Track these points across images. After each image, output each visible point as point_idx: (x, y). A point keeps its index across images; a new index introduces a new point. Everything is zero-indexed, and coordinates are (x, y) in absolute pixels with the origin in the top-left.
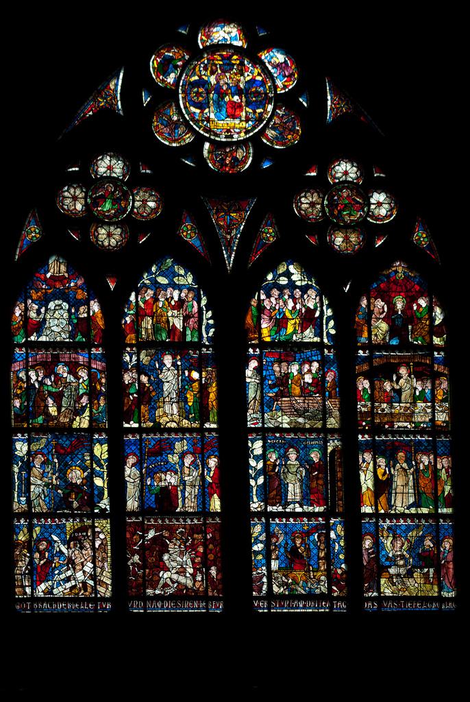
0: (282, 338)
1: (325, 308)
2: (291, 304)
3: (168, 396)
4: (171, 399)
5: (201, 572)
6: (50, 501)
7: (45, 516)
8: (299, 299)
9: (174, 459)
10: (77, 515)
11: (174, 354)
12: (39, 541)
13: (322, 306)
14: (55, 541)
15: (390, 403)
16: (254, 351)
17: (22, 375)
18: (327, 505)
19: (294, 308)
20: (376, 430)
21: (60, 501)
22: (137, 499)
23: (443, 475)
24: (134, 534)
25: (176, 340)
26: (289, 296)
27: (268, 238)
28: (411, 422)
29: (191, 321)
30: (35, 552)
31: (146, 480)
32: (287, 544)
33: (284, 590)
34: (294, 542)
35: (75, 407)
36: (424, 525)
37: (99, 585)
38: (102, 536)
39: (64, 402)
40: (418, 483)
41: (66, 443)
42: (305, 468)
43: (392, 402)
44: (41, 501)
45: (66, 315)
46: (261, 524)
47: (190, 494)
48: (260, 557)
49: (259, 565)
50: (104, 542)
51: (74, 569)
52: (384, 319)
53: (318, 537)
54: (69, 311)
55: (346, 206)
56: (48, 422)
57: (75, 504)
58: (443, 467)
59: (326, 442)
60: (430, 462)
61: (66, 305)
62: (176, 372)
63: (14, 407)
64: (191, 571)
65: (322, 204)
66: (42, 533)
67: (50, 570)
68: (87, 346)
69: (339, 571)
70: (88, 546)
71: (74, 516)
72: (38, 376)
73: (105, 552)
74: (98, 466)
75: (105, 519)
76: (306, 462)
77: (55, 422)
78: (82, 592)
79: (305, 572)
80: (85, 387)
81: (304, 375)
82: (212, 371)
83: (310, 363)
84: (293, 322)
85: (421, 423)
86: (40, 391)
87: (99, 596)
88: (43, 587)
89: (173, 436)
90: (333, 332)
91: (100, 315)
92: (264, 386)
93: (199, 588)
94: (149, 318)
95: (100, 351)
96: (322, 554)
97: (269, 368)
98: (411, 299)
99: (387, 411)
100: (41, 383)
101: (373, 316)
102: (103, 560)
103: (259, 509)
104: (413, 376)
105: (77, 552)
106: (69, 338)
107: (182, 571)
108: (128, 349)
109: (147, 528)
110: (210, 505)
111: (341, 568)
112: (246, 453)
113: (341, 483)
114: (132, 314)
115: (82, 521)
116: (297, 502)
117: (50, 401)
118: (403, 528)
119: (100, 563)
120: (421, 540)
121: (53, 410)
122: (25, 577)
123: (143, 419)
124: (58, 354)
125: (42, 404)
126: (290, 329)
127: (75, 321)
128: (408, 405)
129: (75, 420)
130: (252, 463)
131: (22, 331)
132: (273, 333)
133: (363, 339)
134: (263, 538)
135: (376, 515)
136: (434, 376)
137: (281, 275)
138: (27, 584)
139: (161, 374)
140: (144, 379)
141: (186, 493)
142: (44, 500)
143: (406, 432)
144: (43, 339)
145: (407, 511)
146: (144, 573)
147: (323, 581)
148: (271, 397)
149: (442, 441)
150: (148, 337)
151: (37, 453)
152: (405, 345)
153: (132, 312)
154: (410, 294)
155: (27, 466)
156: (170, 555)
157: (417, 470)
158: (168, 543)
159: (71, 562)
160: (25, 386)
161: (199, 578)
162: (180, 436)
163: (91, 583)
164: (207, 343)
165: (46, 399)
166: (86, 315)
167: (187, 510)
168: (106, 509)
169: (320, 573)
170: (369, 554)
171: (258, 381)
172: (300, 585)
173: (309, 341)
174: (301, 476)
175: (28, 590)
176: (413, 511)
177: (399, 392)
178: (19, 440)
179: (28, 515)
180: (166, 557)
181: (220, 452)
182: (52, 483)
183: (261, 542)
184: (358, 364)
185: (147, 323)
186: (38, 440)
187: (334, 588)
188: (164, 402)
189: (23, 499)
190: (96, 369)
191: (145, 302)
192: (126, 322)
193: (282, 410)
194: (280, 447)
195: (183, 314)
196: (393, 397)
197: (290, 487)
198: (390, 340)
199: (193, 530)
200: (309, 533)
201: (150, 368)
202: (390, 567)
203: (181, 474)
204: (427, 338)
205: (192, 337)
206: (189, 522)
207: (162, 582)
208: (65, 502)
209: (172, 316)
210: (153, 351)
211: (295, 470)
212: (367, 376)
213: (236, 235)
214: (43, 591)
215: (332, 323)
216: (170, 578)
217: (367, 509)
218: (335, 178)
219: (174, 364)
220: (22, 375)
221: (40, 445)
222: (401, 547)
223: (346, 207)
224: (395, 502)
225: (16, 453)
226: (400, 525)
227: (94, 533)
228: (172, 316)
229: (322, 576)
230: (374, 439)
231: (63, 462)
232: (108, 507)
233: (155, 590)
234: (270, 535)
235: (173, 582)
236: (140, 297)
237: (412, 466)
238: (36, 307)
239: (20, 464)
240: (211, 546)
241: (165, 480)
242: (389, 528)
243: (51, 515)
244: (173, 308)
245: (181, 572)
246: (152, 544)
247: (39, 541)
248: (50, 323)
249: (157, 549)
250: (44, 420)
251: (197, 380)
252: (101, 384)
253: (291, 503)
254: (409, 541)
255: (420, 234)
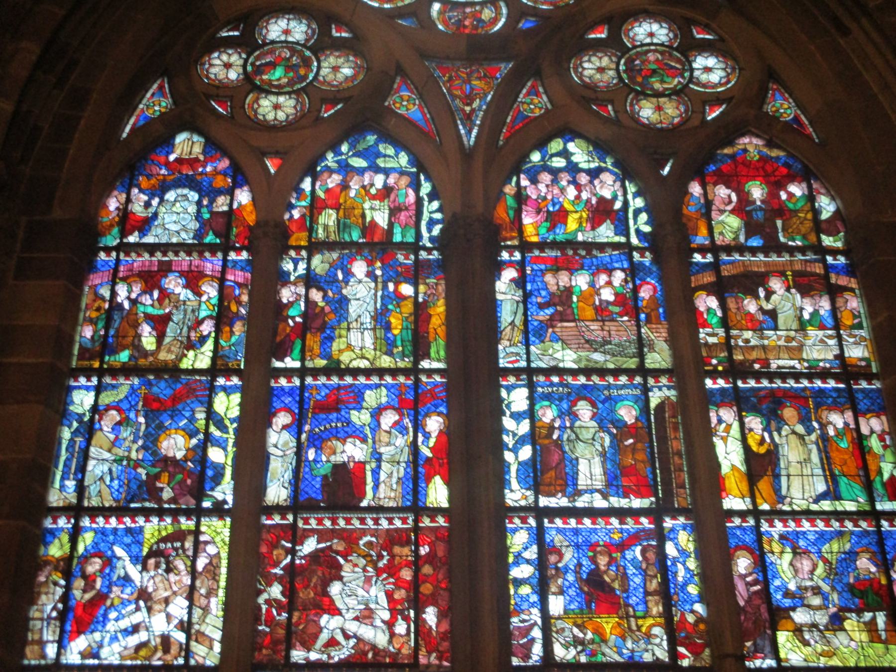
0: (560, 238)
1: (630, 197)
2: (572, 192)
3: (356, 320)
4: (362, 324)
5: (406, 619)
6: (120, 486)
7: (105, 512)
8: (585, 185)
9: (362, 417)
10: (170, 512)
11: (372, 261)
12: (86, 558)
13: (625, 193)
14: (119, 559)
15: (758, 328)
16: (511, 255)
17: (105, 292)
18: (656, 495)
19: (578, 197)
20: (735, 371)
21: (140, 487)
22: (286, 485)
23: (875, 444)
24: (275, 545)
25: (376, 240)
26: (569, 182)
27: (532, 111)
28: (801, 360)
29: (403, 216)
30: (76, 577)
31: (307, 453)
32: (579, 565)
33: (578, 653)
34: (593, 560)
35: (189, 337)
36: (852, 533)
37: (197, 641)
38: (211, 550)
39: (171, 330)
40: (828, 458)
41: (162, 389)
42: (610, 433)
43: (762, 330)
44: (103, 487)
45: (192, 209)
46: (528, 529)
47: (390, 476)
48: (525, 590)
49: (525, 606)
50: (215, 561)
51: (149, 610)
52: (732, 212)
53: (643, 552)
54: (199, 203)
55: (654, 72)
56: (136, 359)
57: (167, 494)
58: (872, 432)
59: (646, 390)
60: (846, 424)
61: (194, 196)
62: (373, 285)
63: (81, 336)
64: (386, 615)
65: (617, 70)
66: (95, 544)
67: (102, 612)
68: (226, 248)
69: (691, 619)
70: (181, 567)
71: (161, 513)
72: (130, 291)
73: (214, 579)
74: (218, 428)
75: (221, 518)
76: (612, 422)
77: (151, 359)
78: (159, 654)
79: (621, 618)
80: (211, 308)
81: (601, 287)
82: (437, 284)
83: (610, 271)
84: (576, 216)
85: (821, 360)
86: (132, 312)
87: (192, 662)
88: (80, 643)
89: (362, 380)
90: (647, 229)
91: (250, 208)
92: (529, 306)
93: (399, 650)
94: (331, 211)
95: (245, 255)
96: (653, 585)
97: (537, 279)
98: (776, 185)
99: (753, 342)
100: (134, 302)
101: (714, 207)
102: (208, 596)
103: (523, 503)
104: (793, 291)
105: (158, 579)
106: (194, 238)
107: (366, 616)
108: (293, 253)
109: (303, 534)
110: (426, 495)
111: (692, 611)
112: (497, 409)
113: (681, 457)
114: (305, 207)
115: (176, 521)
116: (598, 491)
117: (146, 329)
118: (811, 537)
119: (202, 599)
120: (851, 556)
121: (148, 342)
122: (48, 624)
123: (308, 354)
124: (171, 261)
125: (131, 332)
126: (572, 224)
127: (206, 216)
128: (792, 334)
129: (186, 356)
130: (508, 423)
131: (115, 231)
132: (543, 231)
133: (701, 239)
134: (532, 553)
135: (756, 513)
136: (834, 292)
137: (552, 156)
138: (51, 638)
139: (346, 288)
140: (316, 296)
141: (382, 473)
142: (109, 487)
143: (797, 376)
144: (149, 239)
145: (814, 507)
146: (289, 619)
147: (657, 636)
148: (541, 321)
149: (863, 391)
150: (328, 237)
151: (108, 408)
152: (772, 246)
153: (303, 203)
154: (772, 179)
155: (89, 430)
156: (344, 584)
157: (824, 438)
158: (342, 561)
159: (143, 595)
160: (107, 306)
161: (401, 628)
162: (375, 380)
163: (181, 637)
164: (429, 245)
165: (139, 324)
166: (225, 208)
167: (381, 503)
168: (225, 502)
169: (650, 621)
170: (749, 585)
171: (517, 299)
172: (611, 644)
173: (605, 240)
174: (602, 446)
175: (51, 651)
176: (826, 505)
177: (773, 314)
178: (79, 388)
179: (76, 511)
180: (335, 589)
181: (448, 408)
182: (129, 459)
183: (528, 562)
184: (694, 274)
185: (328, 218)
186: (114, 387)
187: (682, 650)
188: (349, 329)
189: (71, 484)
190: (234, 282)
191: (328, 191)
192: (292, 216)
193: (563, 341)
194: (561, 399)
195: (389, 206)
196: (761, 322)
197: (583, 466)
198: (746, 240)
199: (392, 539)
200: (623, 546)
201: (328, 279)
202: (793, 609)
203: (374, 442)
204: (813, 238)
205: (403, 236)
206: (384, 524)
207: (324, 637)
208: (150, 489)
209: (372, 208)
210: (335, 255)
211: (590, 436)
212: (711, 289)
213: (480, 107)
214: (80, 653)
215: (644, 217)
216: (343, 631)
217: (733, 502)
218: (633, 39)
219: (370, 274)
220: (105, 292)
221: (118, 394)
222: (812, 572)
223: (654, 72)
224: (789, 487)
225: (71, 408)
226: (805, 533)
227: (197, 544)
228: (372, 208)
229: (654, 625)
230: (736, 387)
231: (154, 421)
232: (230, 499)
233: (309, 650)
234: (545, 550)
235: (347, 637)
236: (318, 184)
237: (814, 430)
238: (146, 198)
239: (75, 425)
240: (427, 569)
241: (344, 451)
242: (783, 537)
243: (119, 511)
244: (373, 198)
245: (365, 617)
246: (310, 564)
247: (86, 558)
248: (164, 219)
249: (320, 573)
250: (131, 357)
251: (410, 297)
252: (239, 303)
253: (586, 491)
254: (826, 561)
255: (778, 105)
